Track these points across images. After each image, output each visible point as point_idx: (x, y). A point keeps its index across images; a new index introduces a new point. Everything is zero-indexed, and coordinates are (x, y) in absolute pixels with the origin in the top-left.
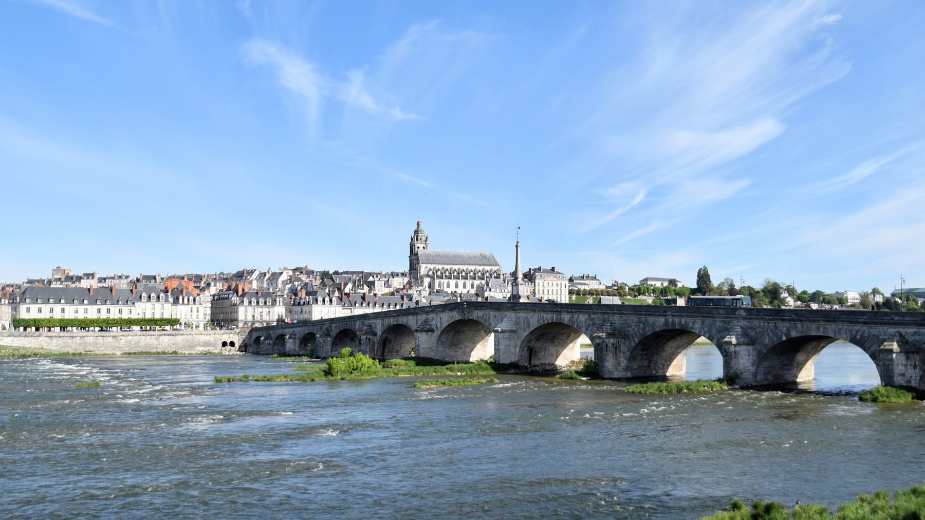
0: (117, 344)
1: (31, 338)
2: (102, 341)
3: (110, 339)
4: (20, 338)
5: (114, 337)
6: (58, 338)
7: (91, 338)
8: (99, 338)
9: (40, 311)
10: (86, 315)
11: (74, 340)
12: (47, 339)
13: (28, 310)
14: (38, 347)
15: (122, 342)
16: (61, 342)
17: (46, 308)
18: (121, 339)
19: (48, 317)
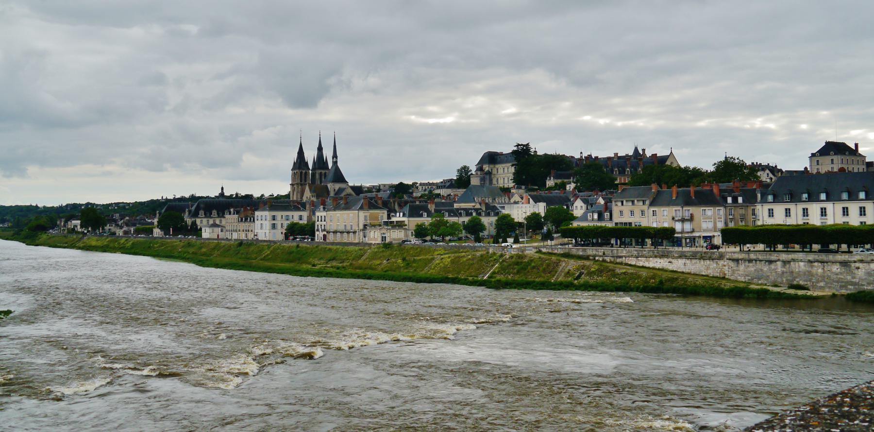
0: (849, 278)
1: (708, 262)
2: (820, 271)
3: (836, 268)
4: (694, 261)
5: (844, 264)
6: (747, 263)
7: (802, 264)
8: (816, 264)
9: (788, 212)
10: (863, 219)
11: (773, 266)
12: (731, 264)
13: (771, 213)
14: (718, 275)
15: (861, 273)
16: (753, 269)
17: (796, 209)
18: (858, 268)
19: (800, 222)
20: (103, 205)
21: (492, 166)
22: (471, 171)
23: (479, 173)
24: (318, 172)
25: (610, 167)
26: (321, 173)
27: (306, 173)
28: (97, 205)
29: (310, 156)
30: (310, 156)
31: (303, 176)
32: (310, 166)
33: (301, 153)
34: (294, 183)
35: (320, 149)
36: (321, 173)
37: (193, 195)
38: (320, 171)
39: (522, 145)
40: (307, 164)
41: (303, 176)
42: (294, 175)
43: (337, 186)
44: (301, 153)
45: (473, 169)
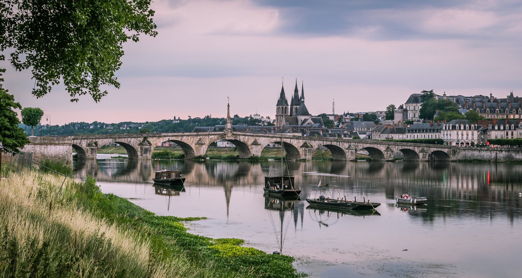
20: (113, 125)
21: (415, 105)
22: (396, 108)
23: (400, 110)
24: (295, 107)
25: (484, 108)
26: (296, 108)
27: (286, 108)
28: (107, 125)
29: (289, 96)
30: (289, 96)
31: (284, 110)
32: (289, 103)
33: (283, 93)
34: (278, 115)
35: (296, 91)
36: (296, 108)
37: (208, 116)
38: (296, 107)
39: (426, 92)
40: (286, 102)
41: (284, 110)
42: (278, 109)
43: (303, 118)
44: (283, 93)
45: (397, 107)
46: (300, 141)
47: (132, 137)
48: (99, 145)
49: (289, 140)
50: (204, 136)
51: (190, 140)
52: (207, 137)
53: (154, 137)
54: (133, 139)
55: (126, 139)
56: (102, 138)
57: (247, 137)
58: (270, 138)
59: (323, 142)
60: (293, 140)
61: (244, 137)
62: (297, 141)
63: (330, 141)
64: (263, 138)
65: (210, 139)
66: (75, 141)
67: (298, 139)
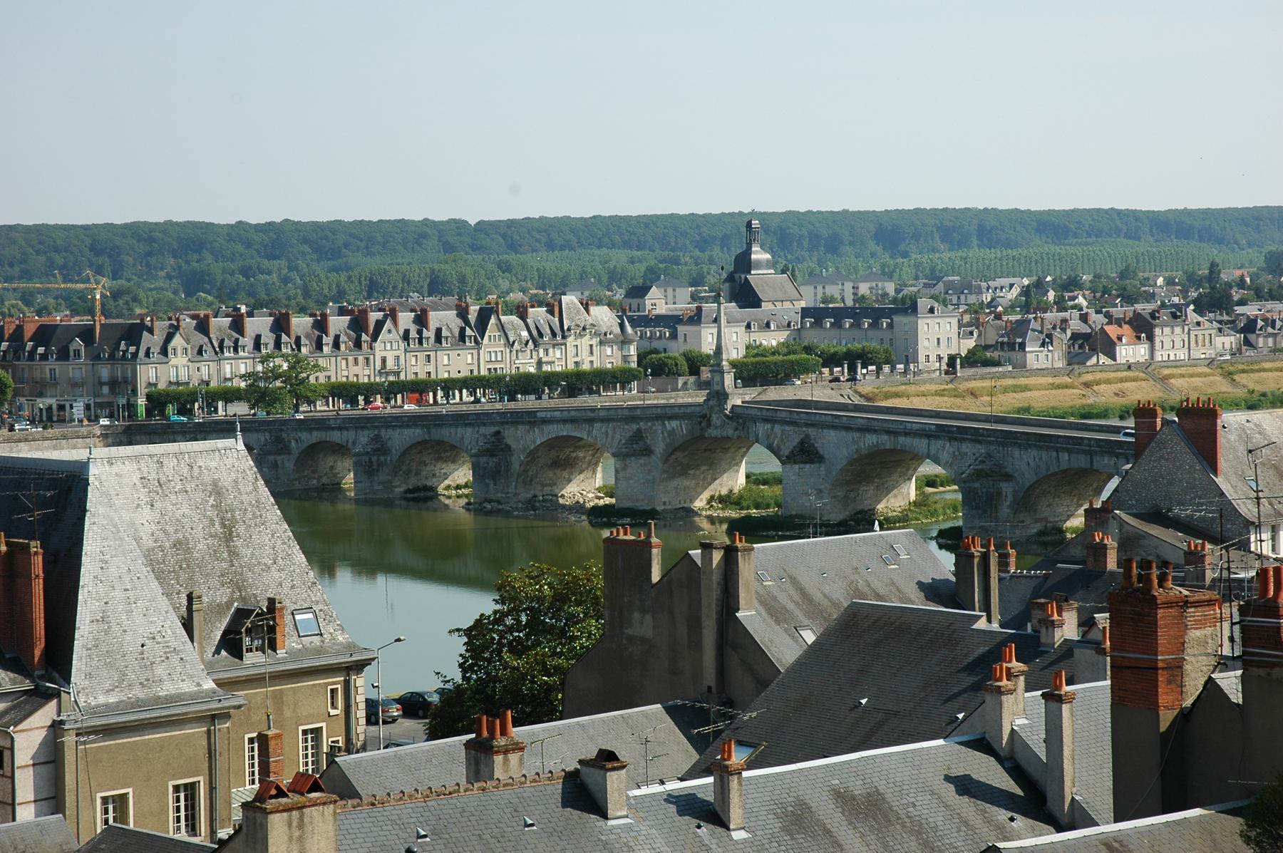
46: (967, 448)
47: (466, 425)
48: (394, 451)
49: (925, 442)
50: (649, 424)
51: (613, 438)
52: (658, 427)
53: (518, 423)
54: (469, 430)
55: (453, 430)
56: (400, 426)
57: (777, 428)
58: (856, 435)
59: (1058, 458)
60: (940, 442)
61: (769, 426)
62: (952, 450)
63: (1084, 452)
64: (833, 433)
65: (669, 436)
66: (345, 433)
67: (955, 439)
